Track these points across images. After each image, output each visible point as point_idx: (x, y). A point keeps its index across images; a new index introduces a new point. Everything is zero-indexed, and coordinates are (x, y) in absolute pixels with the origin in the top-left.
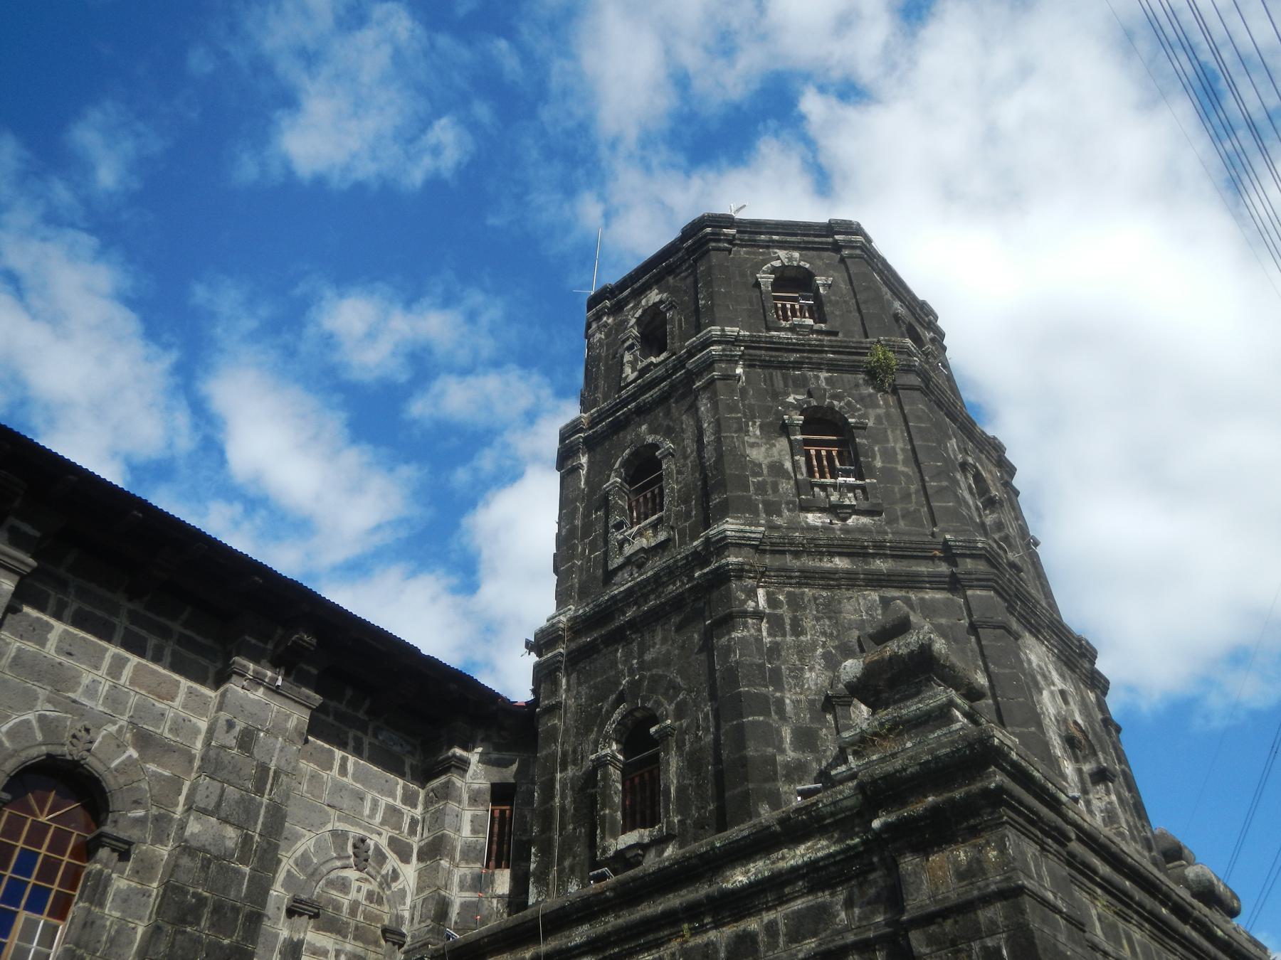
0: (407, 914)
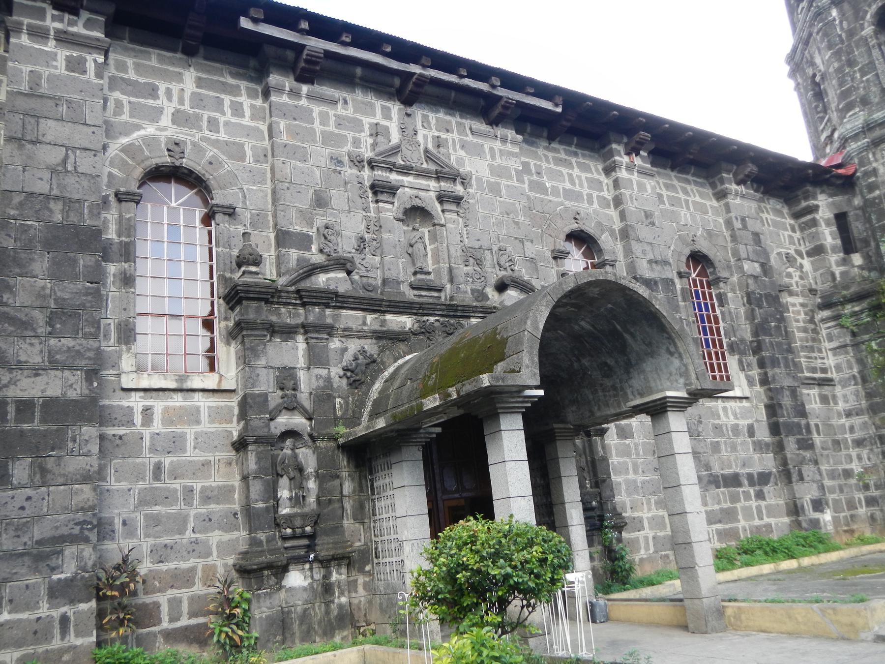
0: (812, 281)
